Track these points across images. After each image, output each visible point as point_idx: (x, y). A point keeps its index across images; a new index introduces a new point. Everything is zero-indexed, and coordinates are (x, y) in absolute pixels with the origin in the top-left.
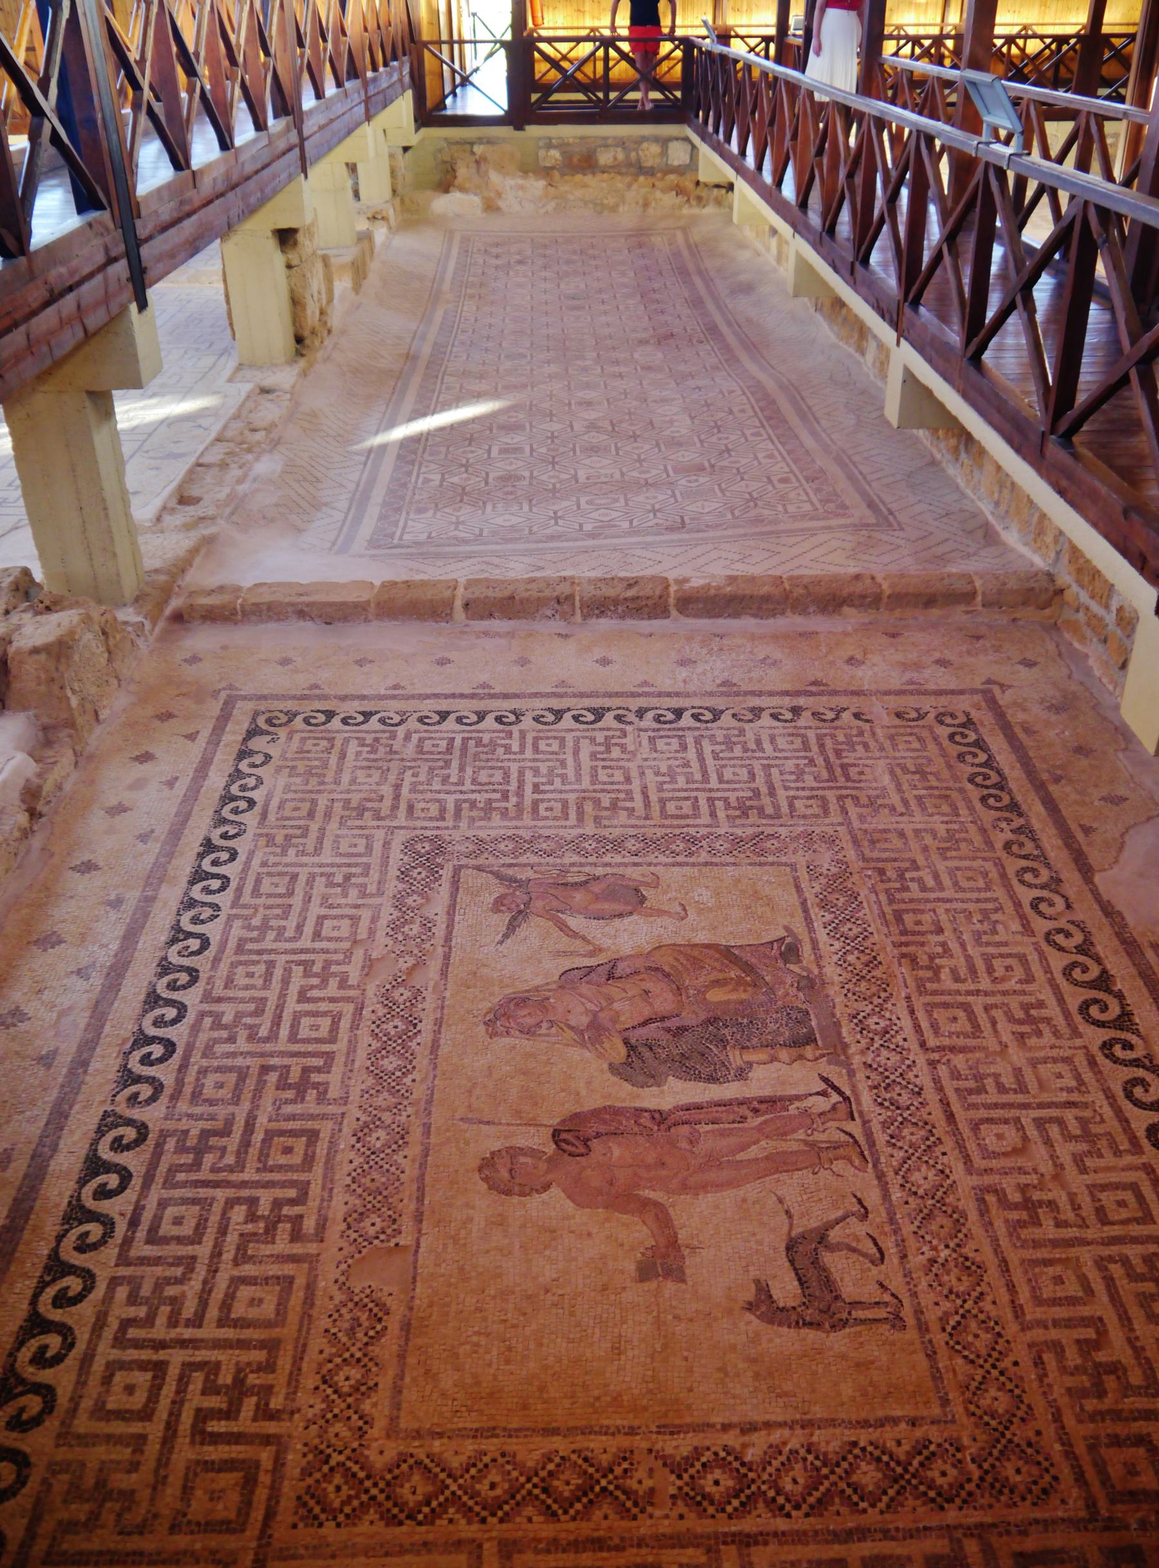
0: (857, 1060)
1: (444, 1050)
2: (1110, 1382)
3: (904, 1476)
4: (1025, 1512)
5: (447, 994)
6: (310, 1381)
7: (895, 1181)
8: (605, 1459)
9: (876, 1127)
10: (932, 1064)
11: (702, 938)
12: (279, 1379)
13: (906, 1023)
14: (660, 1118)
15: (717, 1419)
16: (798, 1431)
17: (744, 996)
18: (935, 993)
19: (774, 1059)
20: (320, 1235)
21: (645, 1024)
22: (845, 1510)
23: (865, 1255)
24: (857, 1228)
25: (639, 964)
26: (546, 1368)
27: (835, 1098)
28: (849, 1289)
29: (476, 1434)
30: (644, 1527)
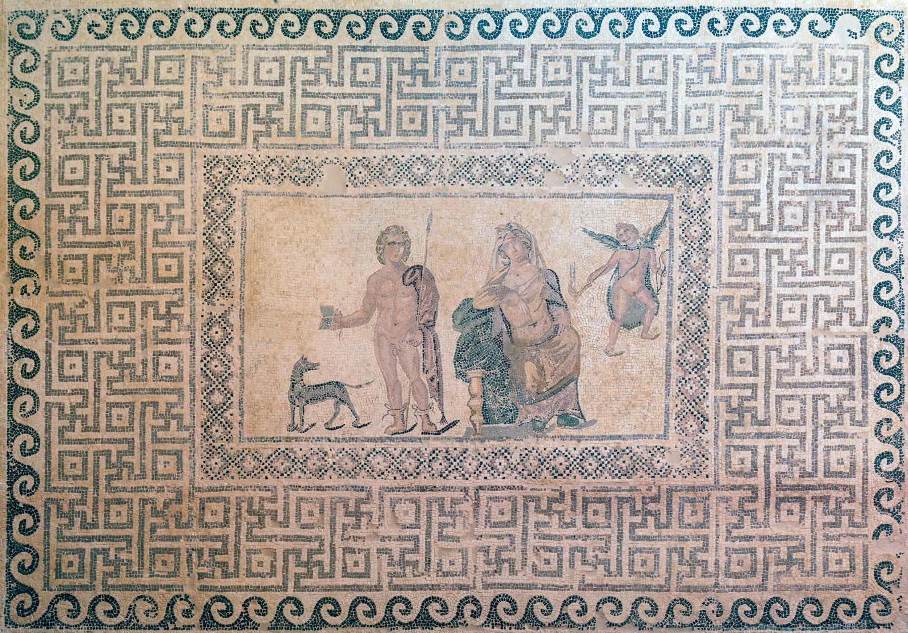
0: (470, 446)
1: (487, 201)
2: (255, 519)
3: (216, 412)
4: (199, 461)
5: (536, 199)
6: (272, 153)
7: (379, 446)
8: (229, 285)
9: (417, 445)
10: (465, 490)
11: (586, 363)
12: (275, 139)
13: (499, 482)
14: (430, 325)
15: (246, 336)
16: (239, 371)
17: (529, 385)
18: (526, 507)
19: (473, 396)
20: (355, 146)
21: (505, 321)
22: (203, 385)
23: (331, 420)
24: (349, 420)
25: (562, 321)
26: (275, 260)
27: (440, 427)
28: (310, 408)
29: (244, 230)
30: (199, 301)
